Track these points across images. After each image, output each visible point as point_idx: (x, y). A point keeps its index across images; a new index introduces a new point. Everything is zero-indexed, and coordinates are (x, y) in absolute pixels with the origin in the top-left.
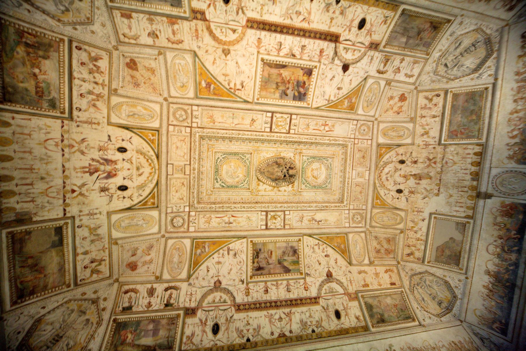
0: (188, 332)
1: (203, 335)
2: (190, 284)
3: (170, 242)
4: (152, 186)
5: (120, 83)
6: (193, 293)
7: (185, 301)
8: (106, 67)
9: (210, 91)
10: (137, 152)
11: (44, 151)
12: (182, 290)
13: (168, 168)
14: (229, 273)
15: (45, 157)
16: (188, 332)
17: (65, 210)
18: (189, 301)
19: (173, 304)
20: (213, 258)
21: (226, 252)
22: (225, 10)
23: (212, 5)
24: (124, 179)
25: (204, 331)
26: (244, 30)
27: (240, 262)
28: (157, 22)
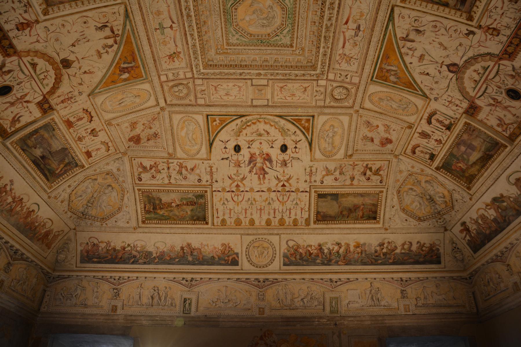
0: (493, 122)
1: (509, 111)
2: (436, 99)
3: (368, 104)
4: (282, 122)
5: (160, 150)
6: (450, 99)
7: (454, 111)
8: (148, 160)
9: (132, 67)
10: (239, 136)
11: (244, 202)
12: (438, 108)
13: (258, 104)
14: (445, 49)
15: (250, 202)
16: (493, 122)
17: (302, 192)
18: (458, 108)
19: (451, 122)
20: (411, 63)
21: (409, 44)
22: (18, 86)
23: (24, 100)
24: (272, 147)
25: (506, 108)
26: (23, 54)
27: (436, 26)
28: (79, 135)
